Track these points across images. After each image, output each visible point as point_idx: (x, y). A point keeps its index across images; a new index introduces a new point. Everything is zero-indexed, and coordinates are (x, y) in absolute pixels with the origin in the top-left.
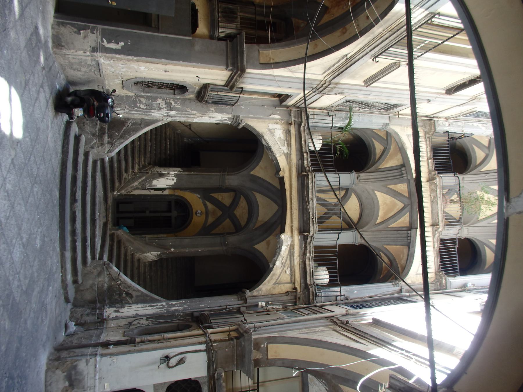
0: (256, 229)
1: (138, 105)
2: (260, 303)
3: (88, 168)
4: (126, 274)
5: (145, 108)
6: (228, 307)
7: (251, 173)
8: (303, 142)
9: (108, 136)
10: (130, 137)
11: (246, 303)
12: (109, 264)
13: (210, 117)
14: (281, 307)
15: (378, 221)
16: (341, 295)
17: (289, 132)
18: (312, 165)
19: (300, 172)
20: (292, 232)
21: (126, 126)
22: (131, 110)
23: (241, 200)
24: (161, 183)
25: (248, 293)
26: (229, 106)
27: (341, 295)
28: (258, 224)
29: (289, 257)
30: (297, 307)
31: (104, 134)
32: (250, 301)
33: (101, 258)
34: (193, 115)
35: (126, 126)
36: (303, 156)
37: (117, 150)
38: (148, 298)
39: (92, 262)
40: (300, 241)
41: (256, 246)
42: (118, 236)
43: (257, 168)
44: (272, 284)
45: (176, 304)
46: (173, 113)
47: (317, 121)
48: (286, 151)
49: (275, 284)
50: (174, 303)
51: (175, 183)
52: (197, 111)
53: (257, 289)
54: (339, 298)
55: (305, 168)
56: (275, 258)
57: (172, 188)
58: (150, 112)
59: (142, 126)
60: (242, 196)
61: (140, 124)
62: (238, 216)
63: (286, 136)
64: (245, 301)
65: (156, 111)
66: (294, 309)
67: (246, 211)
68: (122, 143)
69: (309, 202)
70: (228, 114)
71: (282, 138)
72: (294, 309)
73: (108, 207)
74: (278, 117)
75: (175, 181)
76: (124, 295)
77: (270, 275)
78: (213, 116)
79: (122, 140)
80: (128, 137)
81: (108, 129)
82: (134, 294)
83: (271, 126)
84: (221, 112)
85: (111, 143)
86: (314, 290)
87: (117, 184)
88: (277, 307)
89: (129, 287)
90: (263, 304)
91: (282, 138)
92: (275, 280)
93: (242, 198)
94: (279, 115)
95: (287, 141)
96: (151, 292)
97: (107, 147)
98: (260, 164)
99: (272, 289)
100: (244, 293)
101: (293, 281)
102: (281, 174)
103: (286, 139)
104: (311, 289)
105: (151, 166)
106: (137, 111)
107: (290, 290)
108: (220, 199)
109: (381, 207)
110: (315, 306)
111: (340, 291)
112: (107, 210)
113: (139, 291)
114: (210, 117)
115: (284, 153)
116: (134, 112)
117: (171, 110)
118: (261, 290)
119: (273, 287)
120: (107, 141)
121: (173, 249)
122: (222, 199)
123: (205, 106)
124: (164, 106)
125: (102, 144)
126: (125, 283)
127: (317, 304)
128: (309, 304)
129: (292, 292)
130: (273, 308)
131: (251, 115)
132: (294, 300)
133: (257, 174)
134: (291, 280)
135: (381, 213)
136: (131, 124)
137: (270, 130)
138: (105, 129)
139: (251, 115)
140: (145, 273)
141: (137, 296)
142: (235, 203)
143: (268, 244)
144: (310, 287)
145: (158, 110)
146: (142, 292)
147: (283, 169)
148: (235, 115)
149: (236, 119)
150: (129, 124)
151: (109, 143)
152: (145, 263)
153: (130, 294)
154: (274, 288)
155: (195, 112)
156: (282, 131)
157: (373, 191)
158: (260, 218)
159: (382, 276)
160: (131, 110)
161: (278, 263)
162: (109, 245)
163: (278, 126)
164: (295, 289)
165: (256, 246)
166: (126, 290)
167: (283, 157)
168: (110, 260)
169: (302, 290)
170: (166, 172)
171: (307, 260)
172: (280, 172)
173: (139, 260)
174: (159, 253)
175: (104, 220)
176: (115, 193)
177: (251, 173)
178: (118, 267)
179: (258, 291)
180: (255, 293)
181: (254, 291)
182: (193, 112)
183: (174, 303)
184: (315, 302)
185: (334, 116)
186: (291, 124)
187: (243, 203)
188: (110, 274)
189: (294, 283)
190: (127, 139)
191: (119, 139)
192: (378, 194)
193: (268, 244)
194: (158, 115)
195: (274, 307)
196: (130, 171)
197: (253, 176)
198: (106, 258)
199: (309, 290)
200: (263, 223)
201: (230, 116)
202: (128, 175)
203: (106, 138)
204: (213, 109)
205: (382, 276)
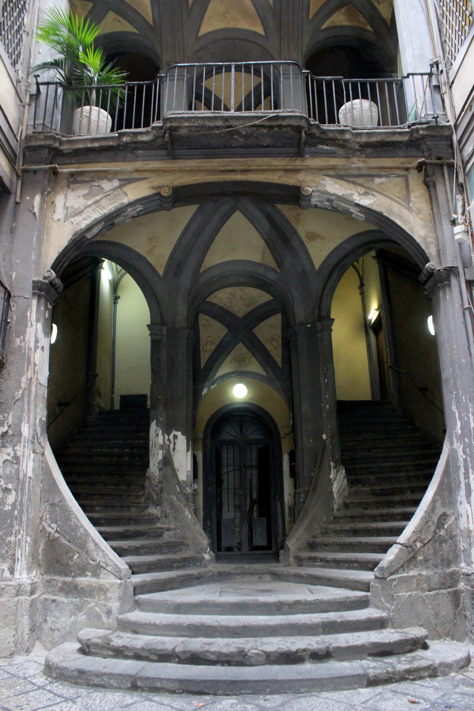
0: (280, 264)
1: (8, 508)
2: (457, 237)
3: (158, 622)
4: (398, 531)
5: (14, 493)
6: (466, 305)
7: (161, 272)
8: (96, 145)
9: (80, 575)
10: (82, 526)
11: (456, 268)
12: (382, 569)
13: (36, 347)
14: (459, 197)
15: (260, 30)
16: (430, 75)
17: (72, 174)
18: (147, 124)
19: (163, 152)
20: (297, 171)
21: (57, 535)
22: (20, 525)
23: (215, 301)
24: (183, 462)
25: (433, 264)
26: (11, 303)
27: (430, 75)
28: (271, 263)
29: (350, 179)
30: (460, 164)
31: (76, 587)
32: (450, 261)
33: (366, 587)
34: (30, 384)
35: (57, 535)
36: (126, 144)
37: (113, 555)
38: (446, 481)
39: (378, 607)
40: (316, 155)
41: (317, 264)
42: (300, 549)
43: (151, 259)
44: (411, 216)
45: (461, 418)
46: (26, 430)
47: (48, 119)
48: (116, 183)
49: (409, 209)
50: (459, 424)
51: (183, 434)
52: (21, 375)
53: (423, 247)
54: (434, 83)
55: (156, 138)
56: (353, 210)
57: (193, 442)
58: (24, 482)
59: (57, 500)
60: (207, 300)
61: (53, 505)
62: (248, 310)
63: (82, 182)
64: (451, 271)
65: (23, 466)
66: (464, 169)
67: (238, 291)
68: (96, 544)
69: (231, 127)
70: (29, 306)
71: (86, 191)
72: (464, 169)
73: (239, 571)
74: (38, 199)
75: (179, 434)
76: (442, 532)
77: (393, 218)
78: (33, 340)
79: (91, 545)
80: (81, 531)
81: (66, 575)
82: (440, 511)
83: (59, 213)
84: (23, 322)
85: (97, 570)
86: (425, 126)
87: (188, 553)
88: (460, 204)
89: (425, 521)
90: (457, 229)
91: (86, 191)
92: (402, 209)
93: (211, 299)
94: (33, 197)
95: (94, 181)
96: (429, 477)
97: (107, 580)
98: (143, 254)
99: (421, 216)
100: (431, 274)
101: (405, 173)
102: (166, 192)
103: (87, 182)
104: (421, 132)
105: (147, 483)
106: (21, 512)
107: (423, 178)
108: (213, 347)
109: (232, 25)
110: (456, 126)
111: (422, 74)
112: (244, 574)
113: (434, 501)
114: (36, 347)
115: (121, 187)
116: (25, 518)
117: (20, 434)
118: (425, 239)
119: (418, 214)
120: (94, 580)
121: (324, 437)
122: (212, 343)
123: (11, 358)
124: (10, 450)
125: (102, 590)
126: (419, 530)
127: (452, 123)
128: (450, 138)
129: (426, 175)
130: (463, 213)
131: (33, 258)
132: (445, 168)
133: (164, 261)
134: (399, 176)
135: (244, 25)
136: (54, 525)
137: (67, 217)
138: (65, 583)
139: (33, 258)
140: (374, 493)
141: (443, 505)
142: (222, 315)
143: (313, 236)
144: (415, 135)
145: (18, 463)
146: (436, 494)
147: (153, 188)
148: (31, 291)
149: (41, 290)
150: (52, 528)
151: (96, 575)
152: (350, 495)
153: (439, 518)
154: (419, 212)
155: (24, 380)
156: (69, 191)
157: (198, 39)
158: (257, 258)
159: (369, 28)
160: (20, 525)
161: (366, 202)
162: (323, 566)
163: (60, 200)
164: (420, 167)
165: (317, 264)
166: (433, 528)
167: (128, 189)
168: (371, 566)
169: (421, 154)
170: (161, 452)
171: (358, 140)
172: (163, 194)
173: (346, 506)
174: (332, 464)
175: (268, 577)
176: (207, 557)
177: (161, 272)
178: (384, 548)
179: (427, 245)
180: (431, 251)
181: (427, 252)
182: (23, 385)
183: (459, 424)
184: (448, 124)
185: (40, 80)
186: (55, 172)
187: (222, 297)
188: (402, 566)
189: (407, 169)
190: (87, 535)
191: (87, 552)
192: (205, 29)
193: (313, 236)
194: (31, 464)
195: (460, 210)
196: (158, 525)
197: (166, 272)
198: (367, 576)
199: (423, 137)
200: (267, 250)
201: (35, 302)
202: (168, 530)
203: (84, 581)
204: (18, 340)
205: (369, 28)
